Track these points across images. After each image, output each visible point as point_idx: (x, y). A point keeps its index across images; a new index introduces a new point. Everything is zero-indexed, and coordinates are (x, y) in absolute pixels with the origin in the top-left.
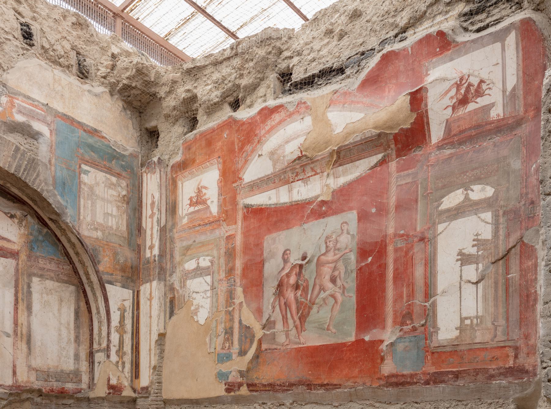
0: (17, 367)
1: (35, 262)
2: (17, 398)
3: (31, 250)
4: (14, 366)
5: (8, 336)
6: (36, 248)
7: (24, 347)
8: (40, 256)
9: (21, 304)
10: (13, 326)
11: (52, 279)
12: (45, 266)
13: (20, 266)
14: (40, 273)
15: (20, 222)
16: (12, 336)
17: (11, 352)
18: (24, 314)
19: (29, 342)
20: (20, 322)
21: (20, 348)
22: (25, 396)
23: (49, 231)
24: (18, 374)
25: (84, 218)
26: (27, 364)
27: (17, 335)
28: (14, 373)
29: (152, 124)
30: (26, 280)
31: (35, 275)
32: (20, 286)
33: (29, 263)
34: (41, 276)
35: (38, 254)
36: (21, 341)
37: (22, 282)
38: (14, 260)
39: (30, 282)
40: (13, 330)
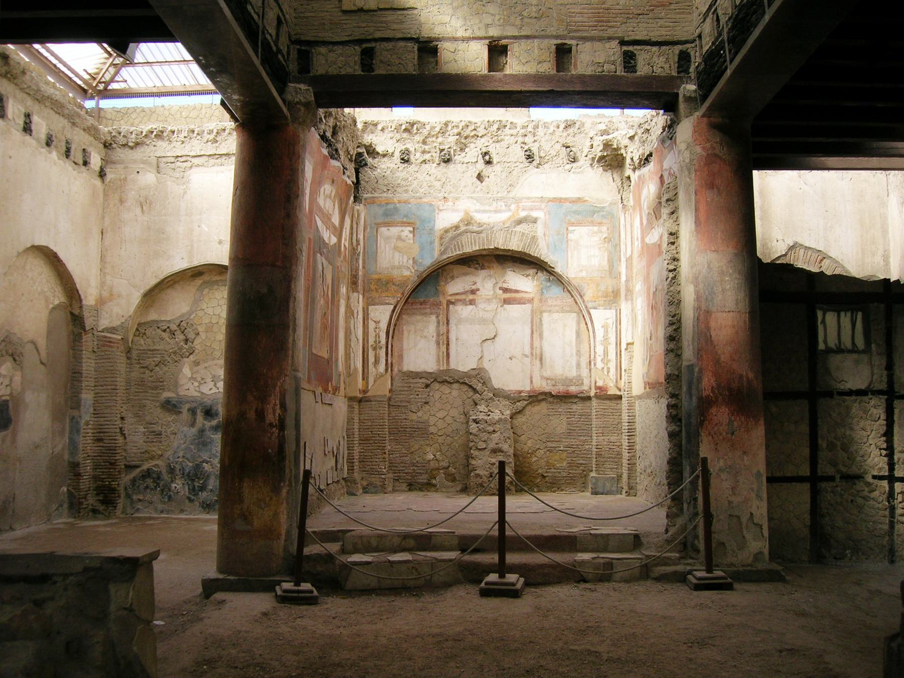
4: (531, 378)
5: (527, 356)
7: (538, 362)
11: (558, 312)
12: (552, 304)
13: (535, 308)
14: (549, 309)
19: (541, 359)
20: (535, 346)
22: (541, 397)
23: (555, 278)
25: (572, 265)
28: (532, 382)
29: (626, 175)
31: (544, 311)
32: (535, 322)
33: (541, 304)
34: (550, 311)
35: (547, 296)
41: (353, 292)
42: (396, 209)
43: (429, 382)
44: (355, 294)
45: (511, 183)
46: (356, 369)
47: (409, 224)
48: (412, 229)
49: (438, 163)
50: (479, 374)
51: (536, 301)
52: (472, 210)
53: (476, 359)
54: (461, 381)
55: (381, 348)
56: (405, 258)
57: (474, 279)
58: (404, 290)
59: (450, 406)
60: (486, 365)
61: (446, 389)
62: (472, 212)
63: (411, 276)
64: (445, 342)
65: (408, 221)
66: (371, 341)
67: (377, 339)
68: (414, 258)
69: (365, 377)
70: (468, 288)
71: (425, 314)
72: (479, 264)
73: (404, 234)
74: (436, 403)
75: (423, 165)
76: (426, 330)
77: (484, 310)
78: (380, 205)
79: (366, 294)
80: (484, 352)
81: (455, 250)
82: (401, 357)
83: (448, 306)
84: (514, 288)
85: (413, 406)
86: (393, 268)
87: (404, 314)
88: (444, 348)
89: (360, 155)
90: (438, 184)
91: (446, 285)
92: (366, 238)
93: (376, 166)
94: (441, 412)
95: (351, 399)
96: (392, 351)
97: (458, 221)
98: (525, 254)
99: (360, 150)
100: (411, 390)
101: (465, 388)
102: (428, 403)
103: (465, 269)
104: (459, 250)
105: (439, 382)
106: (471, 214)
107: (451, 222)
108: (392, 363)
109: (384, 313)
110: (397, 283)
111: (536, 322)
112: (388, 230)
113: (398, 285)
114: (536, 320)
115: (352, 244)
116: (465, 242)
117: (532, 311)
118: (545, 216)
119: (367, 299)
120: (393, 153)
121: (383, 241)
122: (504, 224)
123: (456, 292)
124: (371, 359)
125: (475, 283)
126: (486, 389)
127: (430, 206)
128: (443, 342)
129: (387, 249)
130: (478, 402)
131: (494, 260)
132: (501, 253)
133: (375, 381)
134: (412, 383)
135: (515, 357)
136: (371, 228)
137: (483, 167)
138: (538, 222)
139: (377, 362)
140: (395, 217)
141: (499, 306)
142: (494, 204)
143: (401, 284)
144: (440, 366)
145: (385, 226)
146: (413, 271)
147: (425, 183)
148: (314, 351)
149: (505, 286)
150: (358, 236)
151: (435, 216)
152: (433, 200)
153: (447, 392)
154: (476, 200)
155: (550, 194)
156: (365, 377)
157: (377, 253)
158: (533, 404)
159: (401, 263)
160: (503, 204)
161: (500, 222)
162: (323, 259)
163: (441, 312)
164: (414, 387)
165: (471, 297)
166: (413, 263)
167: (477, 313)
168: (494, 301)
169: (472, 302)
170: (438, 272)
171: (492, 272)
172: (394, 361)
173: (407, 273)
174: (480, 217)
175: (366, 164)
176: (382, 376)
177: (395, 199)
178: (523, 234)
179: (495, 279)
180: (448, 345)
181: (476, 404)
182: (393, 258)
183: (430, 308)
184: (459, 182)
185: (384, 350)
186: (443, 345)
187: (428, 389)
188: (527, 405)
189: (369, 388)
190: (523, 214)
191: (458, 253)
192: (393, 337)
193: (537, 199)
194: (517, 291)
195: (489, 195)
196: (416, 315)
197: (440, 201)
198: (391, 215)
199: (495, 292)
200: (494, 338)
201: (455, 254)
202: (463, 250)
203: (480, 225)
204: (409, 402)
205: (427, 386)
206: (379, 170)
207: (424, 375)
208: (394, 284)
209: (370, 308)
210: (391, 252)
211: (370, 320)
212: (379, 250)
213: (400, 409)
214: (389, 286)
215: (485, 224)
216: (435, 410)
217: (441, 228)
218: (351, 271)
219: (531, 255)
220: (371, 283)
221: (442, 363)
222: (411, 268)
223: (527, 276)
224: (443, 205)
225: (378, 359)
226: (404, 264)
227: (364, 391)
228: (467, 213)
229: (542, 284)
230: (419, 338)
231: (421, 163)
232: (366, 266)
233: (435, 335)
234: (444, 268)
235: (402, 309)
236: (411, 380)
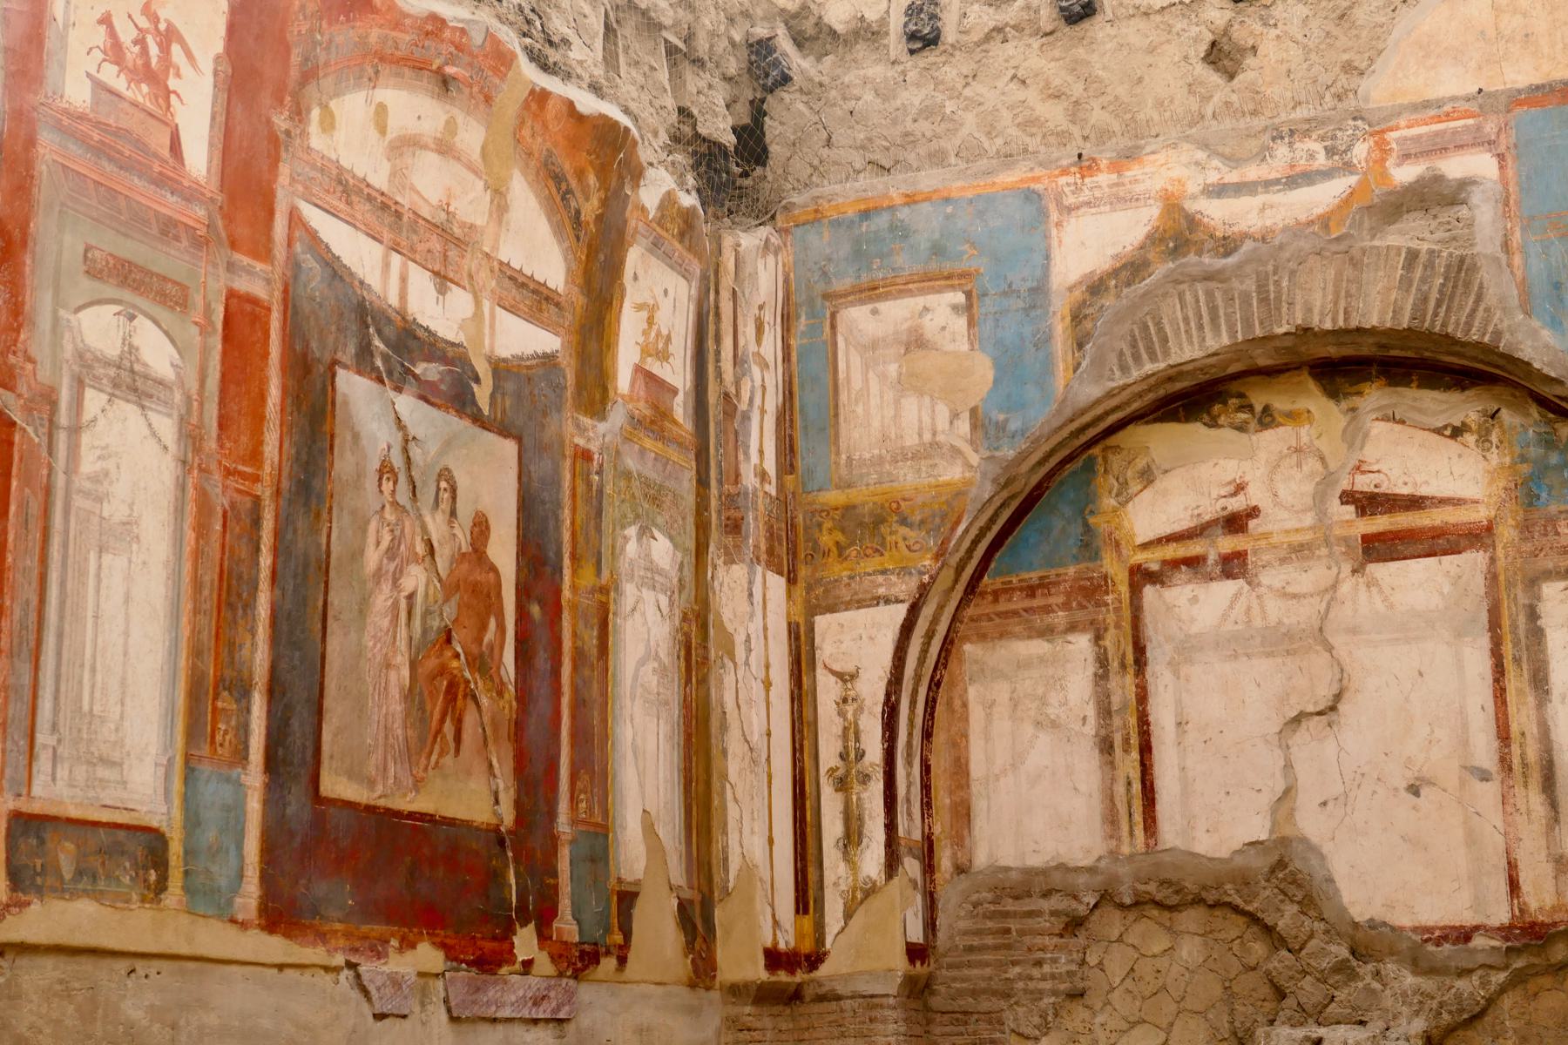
0: (1521, 866)
1: (1546, 535)
2: (1535, 961)
3: (1531, 504)
4: (1512, 866)
5: (1485, 777)
6: (1544, 495)
8: (1561, 512)
9: (1512, 674)
10: (1496, 744)
15: (1484, 439)
16: (1495, 776)
17: (1499, 824)
18: (1525, 703)
19: (1549, 783)
20: (1514, 728)
21: (1523, 809)
24: (1526, 886)
26: (1549, 855)
27: (1510, 769)
28: (1514, 886)
30: (1523, 599)
31: (1548, 575)
32: (1506, 623)
33: (1528, 547)
35: (1553, 508)
36: (1526, 785)
37: (1509, 608)
38: (1481, 552)
39: (1535, 602)
40: (1496, 758)
41: (730, 561)
42: (901, 232)
43: (1082, 910)
44: (739, 571)
45: (1346, 57)
46: (748, 869)
47: (948, 280)
48: (960, 298)
49: (1049, 28)
50: (1281, 864)
51: (1507, 533)
52: (1193, 187)
53: (1266, 799)
54: (1211, 897)
55: (865, 779)
56: (943, 412)
57: (1230, 469)
58: (945, 542)
59: (1173, 1007)
60: (1310, 824)
61: (1149, 935)
62: (1194, 197)
63: (968, 483)
64: (1135, 740)
65: (948, 267)
66: (829, 754)
67: (851, 744)
68: (974, 412)
69: (806, 897)
70: (1211, 510)
71: (1047, 633)
72: (1250, 408)
73: (930, 325)
74: (1115, 997)
75: (996, 48)
76: (1054, 698)
77: (1285, 595)
78: (836, 224)
79: (803, 572)
80: (1298, 767)
81: (1137, 358)
82: (963, 814)
83: (1135, 590)
84: (1405, 491)
85: (1021, 1010)
86: (901, 456)
87: (966, 639)
88: (1129, 764)
89: (761, 49)
90: (1055, 114)
91: (1123, 504)
92: (794, 358)
93: (826, 80)
94: (1138, 1032)
95: (735, 991)
96: (926, 788)
97: (1136, 244)
98: (1429, 335)
99: (761, 31)
100: (1008, 947)
101: (1233, 927)
102: (1080, 995)
103: (1192, 434)
104: (1153, 357)
105: (1121, 906)
106: (1191, 206)
107: (1111, 251)
108: (929, 842)
109: (871, 638)
110: (917, 518)
111: (1514, 627)
112: (875, 312)
113: (922, 522)
114: (1513, 615)
115: (719, 374)
116: (1174, 322)
117: (1492, 578)
118: (1501, 168)
119: (809, 589)
120: (883, 21)
121: (856, 360)
122: (1326, 226)
123: (1168, 530)
124: (832, 828)
125: (1240, 488)
126: (1319, 926)
127: (1027, 198)
128: (1126, 741)
129: (874, 387)
130: (1288, 986)
131: (1311, 384)
132: (1332, 351)
133: (848, 915)
134: (1014, 915)
135: (1431, 783)
136: (812, 315)
137: (1228, 14)
138: (1476, 197)
139: (852, 838)
140: (901, 260)
141: (1347, 568)
142: (1282, 150)
143: (934, 516)
144: (1119, 839)
145: (862, 302)
146: (974, 459)
147: (1006, 115)
148: (335, 785)
149: (1364, 484)
150: (741, 342)
151: (1047, 237)
152: (1038, 172)
153: (1157, 949)
154: (1204, 145)
155: (1521, 74)
156: (806, 897)
157: (836, 406)
158: (1532, 986)
159: (927, 437)
160: (1318, 147)
161: (1310, 223)
162: (406, 404)
163: (1111, 618)
164: (1022, 933)
165: (1227, 544)
166: (974, 427)
167: (1256, 610)
168: (1324, 551)
169: (1233, 566)
170: (1092, 459)
171: (1305, 433)
172: (937, 829)
173: (952, 473)
174: (1217, 213)
175: (786, 79)
176: (870, 891)
177: (893, 193)
178: (1413, 255)
179: (1322, 459)
180: (1146, 749)
181: (1281, 994)
182: (896, 416)
183: (1066, 606)
184: (1138, 90)
185: (877, 787)
186: (1126, 751)
187: (1082, 940)
188: (1503, 990)
189: (828, 945)
190: (1405, 174)
191: (1149, 367)
192: (927, 735)
193: (1466, 106)
194: (1415, 503)
195: (1258, 123)
196: (1018, 637)
197: (1065, 172)
198: (882, 256)
199: (1322, 514)
200: (1333, 708)
201: (1136, 374)
202: (1166, 353)
203: (1227, 245)
204: (1007, 996)
205: (1074, 924)
206: (833, 93)
207: (1057, 879)
208: (904, 521)
209: (821, 621)
210: (890, 395)
211: (820, 671)
212: (843, 397)
213: (971, 1028)
214: (884, 529)
215: (1245, 236)
216: (1112, 1025)
217: (1074, 277)
218: (720, 482)
219: (1455, 342)
220: (820, 525)
221: (1125, 827)
222: (967, 449)
223: (1457, 432)
224: (1077, 190)
225: (854, 825)
226: (941, 438)
227: (808, 957)
228: (1172, 205)
229: (1523, 459)
230: (1028, 729)
231: (988, 38)
232: (800, 464)
233: (1091, 711)
234: (1112, 441)
235: (955, 619)
236: (1010, 905)
